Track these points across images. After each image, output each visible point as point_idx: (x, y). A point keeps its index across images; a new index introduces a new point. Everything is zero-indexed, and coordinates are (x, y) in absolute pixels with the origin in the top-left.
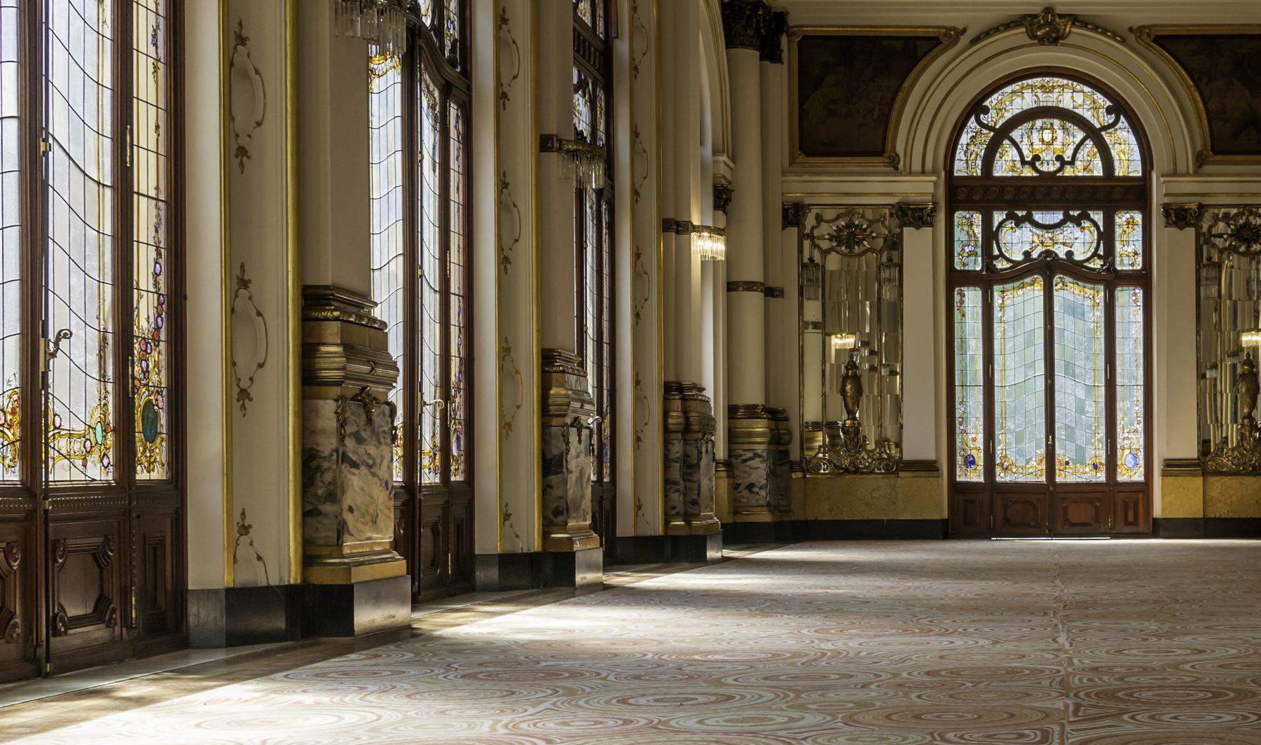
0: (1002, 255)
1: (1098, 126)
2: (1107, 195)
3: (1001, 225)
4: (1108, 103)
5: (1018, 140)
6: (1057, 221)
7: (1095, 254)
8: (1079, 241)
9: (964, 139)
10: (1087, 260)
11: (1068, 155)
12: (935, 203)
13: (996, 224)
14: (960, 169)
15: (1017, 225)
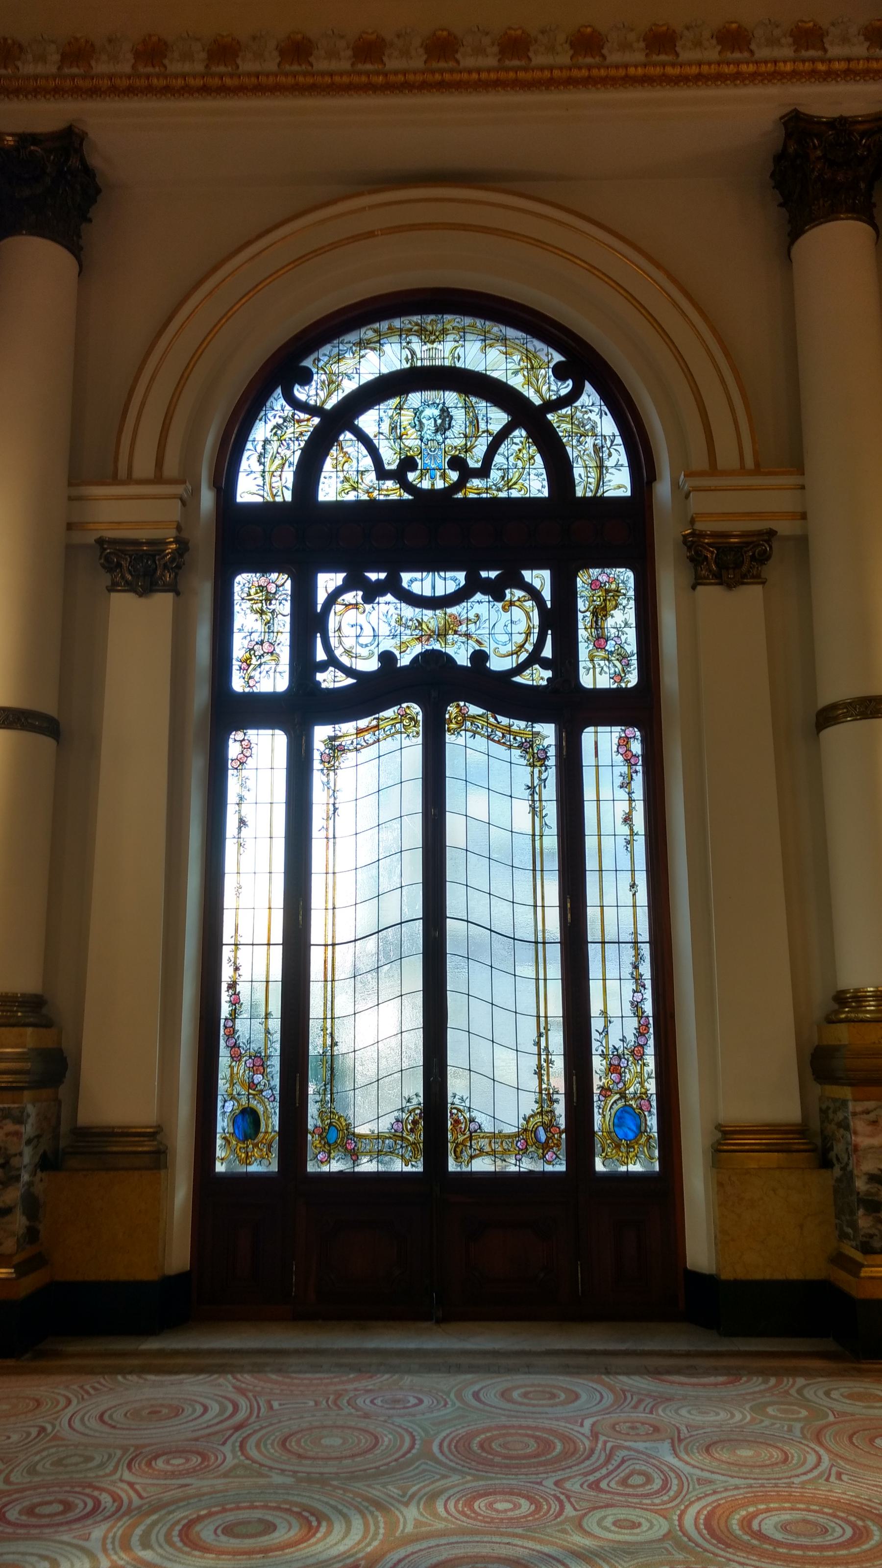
0: (332, 661)
1: (537, 402)
2: (563, 534)
3: (333, 598)
4: (558, 358)
6: (451, 587)
7: (535, 658)
8: (500, 630)
10: (520, 669)
11: (474, 463)
12: (183, 546)
13: (321, 597)
14: (249, 489)
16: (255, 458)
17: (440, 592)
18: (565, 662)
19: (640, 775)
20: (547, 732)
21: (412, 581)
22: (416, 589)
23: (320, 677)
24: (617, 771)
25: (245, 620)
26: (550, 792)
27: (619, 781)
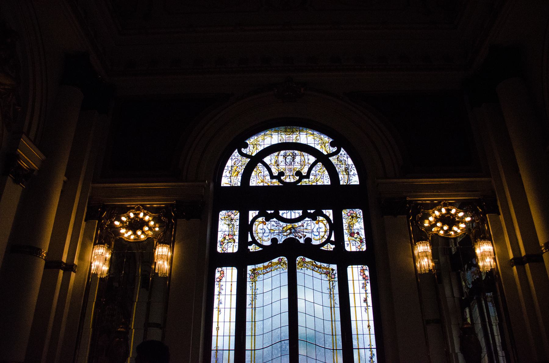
0: (254, 241)
1: (325, 153)
6: (297, 216)
7: (328, 241)
8: (316, 230)
10: (323, 244)
13: (250, 218)
14: (225, 182)
16: (228, 172)
17: (293, 217)
18: (340, 242)
19: (369, 284)
20: (334, 267)
22: (285, 216)
23: (249, 247)
26: (336, 290)
27: (361, 286)
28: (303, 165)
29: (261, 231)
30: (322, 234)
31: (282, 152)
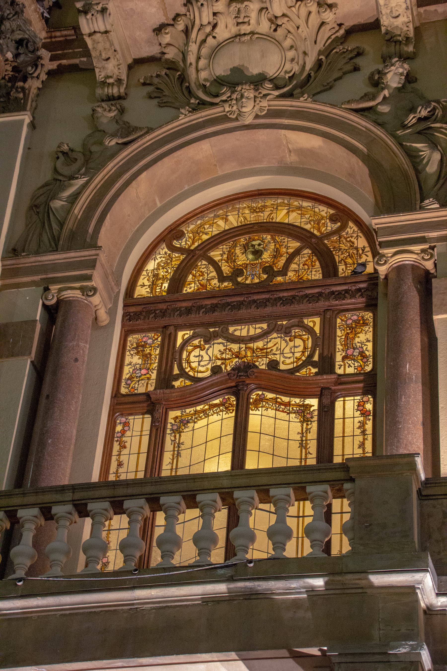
0: (183, 374)
3: (186, 342)
4: (332, 212)
5: (217, 259)
8: (289, 351)
9: (151, 266)
10: (298, 369)
15: (206, 342)
18: (326, 365)
19: (371, 421)
20: (314, 402)
21: (235, 330)
22: (237, 333)
24: (357, 420)
25: (133, 359)
27: (357, 425)
28: (277, 254)
29: (197, 359)
30: (298, 355)
31: (242, 240)
